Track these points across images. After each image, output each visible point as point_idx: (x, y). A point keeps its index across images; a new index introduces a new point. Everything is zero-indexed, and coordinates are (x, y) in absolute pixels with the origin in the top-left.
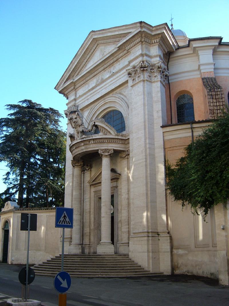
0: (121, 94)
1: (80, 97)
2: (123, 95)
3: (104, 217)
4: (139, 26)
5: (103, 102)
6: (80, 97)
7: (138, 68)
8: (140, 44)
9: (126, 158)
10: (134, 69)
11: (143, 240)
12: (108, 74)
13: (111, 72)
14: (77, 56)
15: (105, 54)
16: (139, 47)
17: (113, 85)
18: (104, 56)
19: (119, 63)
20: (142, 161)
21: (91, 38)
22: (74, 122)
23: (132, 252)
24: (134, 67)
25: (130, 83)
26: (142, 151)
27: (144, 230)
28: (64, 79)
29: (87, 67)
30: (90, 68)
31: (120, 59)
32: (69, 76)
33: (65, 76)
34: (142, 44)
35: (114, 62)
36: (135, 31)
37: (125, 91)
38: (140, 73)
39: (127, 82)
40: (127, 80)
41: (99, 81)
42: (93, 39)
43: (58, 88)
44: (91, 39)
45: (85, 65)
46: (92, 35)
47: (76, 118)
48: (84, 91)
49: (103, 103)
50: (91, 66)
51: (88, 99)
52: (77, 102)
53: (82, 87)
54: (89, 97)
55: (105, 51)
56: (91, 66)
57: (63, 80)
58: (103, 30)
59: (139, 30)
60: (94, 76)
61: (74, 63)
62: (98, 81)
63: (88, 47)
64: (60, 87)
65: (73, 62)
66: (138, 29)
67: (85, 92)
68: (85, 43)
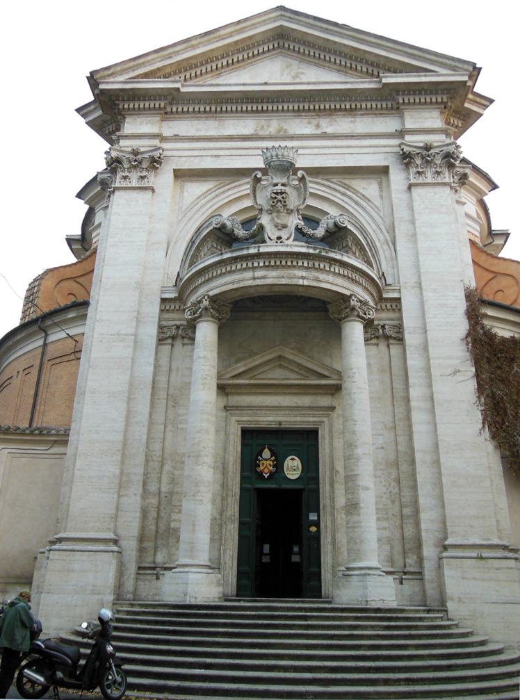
0: (348, 187)
1: (176, 138)
2: (356, 192)
3: (367, 489)
4: (466, 70)
6: (176, 138)
7: (438, 154)
8: (439, 108)
9: (375, 344)
10: (425, 152)
11: (502, 568)
12: (306, 127)
13: (318, 126)
14: (212, 36)
15: (304, 80)
16: (436, 114)
17: (329, 156)
18: (297, 80)
19: (353, 119)
21: (275, 21)
22: (277, 193)
24: (428, 148)
25: (397, 178)
27: (489, 539)
28: (139, 66)
29: (222, 78)
32: (159, 69)
33: (148, 62)
34: (441, 113)
35: (340, 109)
36: (444, 76)
37: (366, 187)
38: (441, 167)
39: (385, 171)
40: (387, 167)
41: (271, 129)
42: (281, 25)
43: (102, 77)
45: (217, 71)
46: (281, 15)
47: (283, 185)
48: (198, 130)
52: (165, 146)
53: (193, 117)
54: (221, 153)
55: (303, 73)
57: (132, 68)
58: (336, 24)
59: (466, 78)
60: (257, 111)
61: (194, 47)
62: (263, 127)
63: (254, 35)
64: (112, 80)
65: (194, 42)
66: (463, 75)
68: (253, 22)
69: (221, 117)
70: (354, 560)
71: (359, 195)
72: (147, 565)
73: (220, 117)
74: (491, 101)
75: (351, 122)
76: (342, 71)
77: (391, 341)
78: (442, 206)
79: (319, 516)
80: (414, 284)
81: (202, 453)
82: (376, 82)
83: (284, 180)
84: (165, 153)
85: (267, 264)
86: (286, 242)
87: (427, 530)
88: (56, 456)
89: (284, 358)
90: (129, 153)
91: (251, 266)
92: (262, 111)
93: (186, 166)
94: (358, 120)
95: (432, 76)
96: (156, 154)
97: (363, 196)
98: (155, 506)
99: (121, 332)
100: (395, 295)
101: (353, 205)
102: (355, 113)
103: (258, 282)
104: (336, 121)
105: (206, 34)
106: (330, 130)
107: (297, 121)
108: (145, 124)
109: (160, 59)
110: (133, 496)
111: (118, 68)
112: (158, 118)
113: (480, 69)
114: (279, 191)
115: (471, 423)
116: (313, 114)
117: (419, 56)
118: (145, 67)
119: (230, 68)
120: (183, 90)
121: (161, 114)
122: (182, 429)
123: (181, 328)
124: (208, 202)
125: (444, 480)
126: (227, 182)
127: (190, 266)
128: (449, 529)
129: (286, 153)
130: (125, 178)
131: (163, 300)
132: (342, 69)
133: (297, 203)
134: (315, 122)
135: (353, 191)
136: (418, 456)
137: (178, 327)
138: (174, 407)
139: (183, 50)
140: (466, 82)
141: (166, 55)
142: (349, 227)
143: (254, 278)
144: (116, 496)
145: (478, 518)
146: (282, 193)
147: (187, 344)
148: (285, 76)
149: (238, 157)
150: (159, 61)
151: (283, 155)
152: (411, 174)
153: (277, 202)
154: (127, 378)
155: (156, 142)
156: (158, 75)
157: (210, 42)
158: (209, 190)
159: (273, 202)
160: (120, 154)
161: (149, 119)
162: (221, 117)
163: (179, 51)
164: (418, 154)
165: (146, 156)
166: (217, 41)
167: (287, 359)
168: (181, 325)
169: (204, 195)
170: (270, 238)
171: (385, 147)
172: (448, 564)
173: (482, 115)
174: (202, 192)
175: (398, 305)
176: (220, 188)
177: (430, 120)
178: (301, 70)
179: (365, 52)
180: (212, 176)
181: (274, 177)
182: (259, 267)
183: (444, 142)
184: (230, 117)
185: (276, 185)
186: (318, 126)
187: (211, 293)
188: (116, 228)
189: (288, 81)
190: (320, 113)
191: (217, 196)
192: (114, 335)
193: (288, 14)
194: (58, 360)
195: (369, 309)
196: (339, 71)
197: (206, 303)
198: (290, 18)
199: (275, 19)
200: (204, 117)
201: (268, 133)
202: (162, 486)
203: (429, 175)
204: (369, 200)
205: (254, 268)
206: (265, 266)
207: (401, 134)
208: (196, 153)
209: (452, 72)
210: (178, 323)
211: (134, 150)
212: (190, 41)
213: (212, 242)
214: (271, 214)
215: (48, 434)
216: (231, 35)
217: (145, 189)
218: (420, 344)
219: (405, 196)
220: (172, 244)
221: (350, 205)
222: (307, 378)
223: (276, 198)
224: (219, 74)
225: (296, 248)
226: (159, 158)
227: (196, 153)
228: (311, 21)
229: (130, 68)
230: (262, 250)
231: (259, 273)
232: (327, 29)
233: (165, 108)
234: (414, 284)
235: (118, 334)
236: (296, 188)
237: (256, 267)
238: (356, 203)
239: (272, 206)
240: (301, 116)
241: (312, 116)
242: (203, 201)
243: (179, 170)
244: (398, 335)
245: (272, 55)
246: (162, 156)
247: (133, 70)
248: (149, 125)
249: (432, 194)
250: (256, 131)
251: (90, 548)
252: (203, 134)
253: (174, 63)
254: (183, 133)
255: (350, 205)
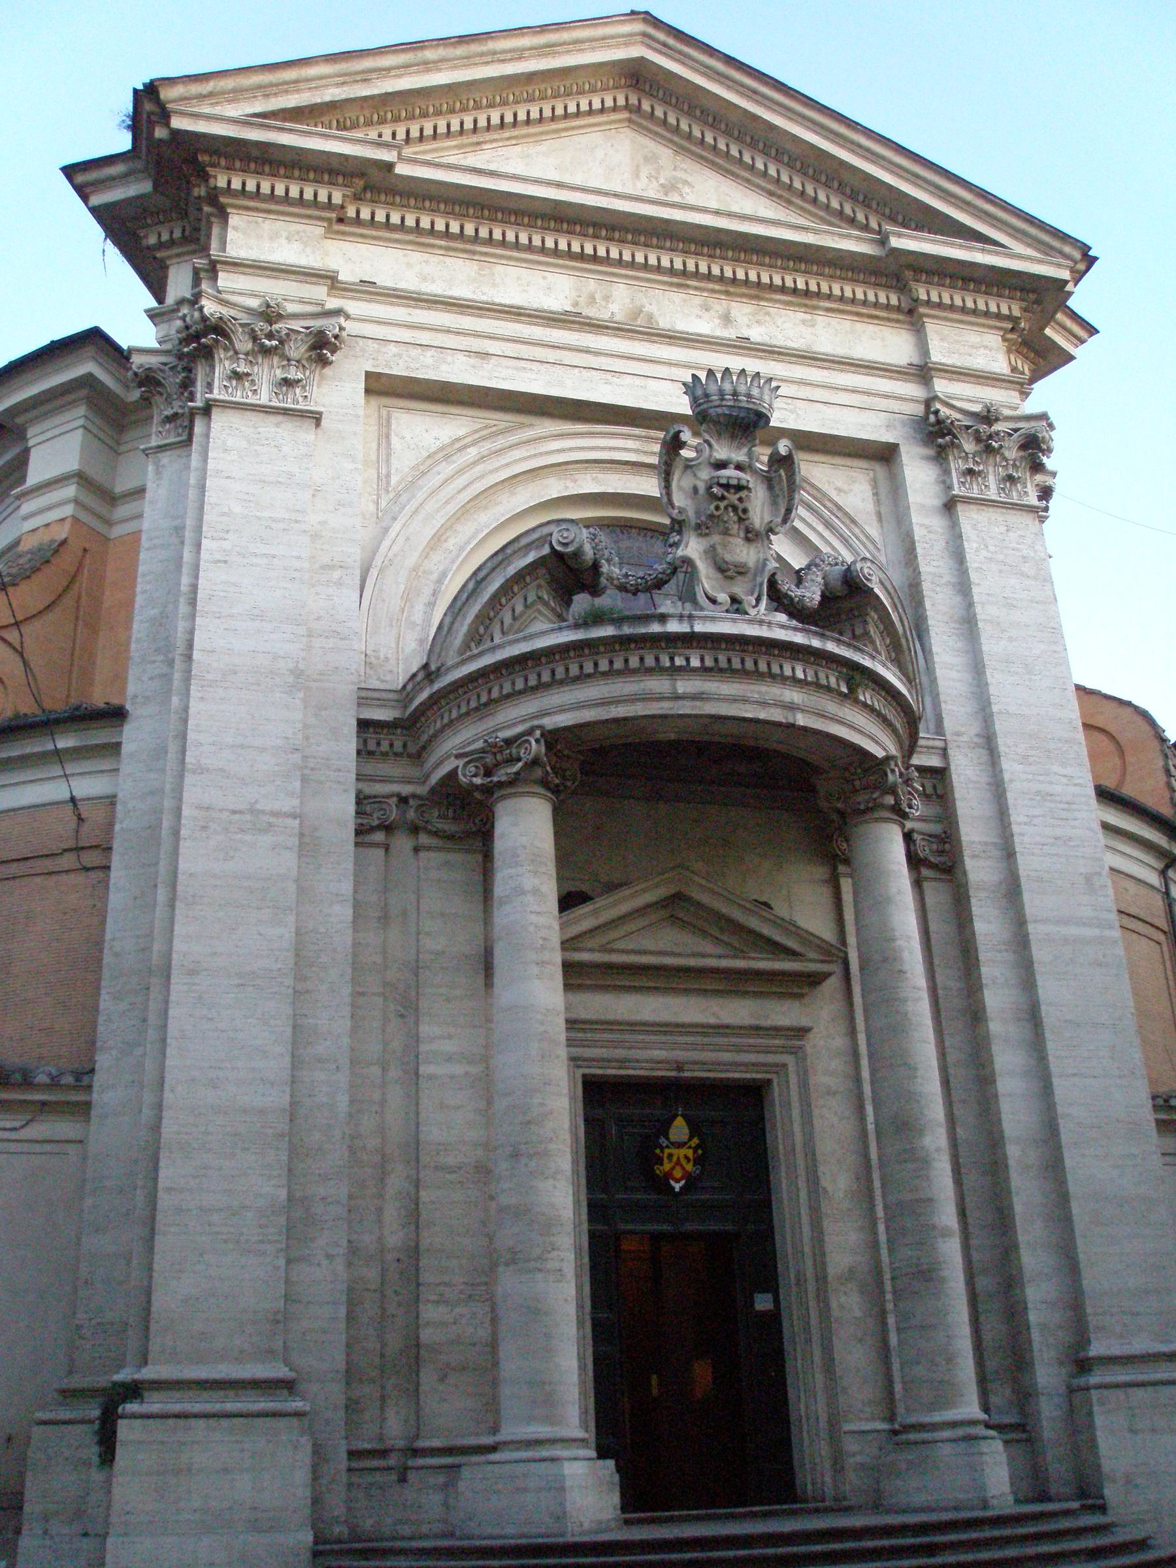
1: (367, 289)
5: (630, 444)
7: (1010, 435)
14: (475, 48)
15: (691, 200)
16: (993, 340)
18: (675, 198)
19: (808, 317)
20: (1096, 932)
21: (626, 44)
22: (727, 487)
23: (1128, 1481)
24: (988, 417)
26: (1088, 879)
30: (492, 174)
31: (827, 304)
32: (332, 106)
33: (308, 80)
37: (845, 487)
38: (1014, 466)
44: (618, 46)
47: (739, 467)
48: (425, 279)
49: (626, 450)
50: (616, 195)
51: (485, 355)
55: (686, 182)
56: (616, 195)
57: (265, 90)
59: (1065, 275)
60: (582, 257)
61: (427, 66)
65: (430, 54)
66: (1059, 266)
67: (456, 292)
69: (486, 254)
70: (933, 1406)
71: (829, 504)
72: (367, 1446)
73: (481, 254)
74: (1097, 332)
75: (804, 322)
76: (780, 197)
77: (925, 872)
78: (1025, 559)
79: (777, 1302)
80: (976, 740)
81: (552, 1146)
82: (872, 241)
83: (740, 456)
84: (351, 327)
85: (709, 662)
86: (753, 612)
87: (1043, 1327)
88: (48, 1147)
89: (688, 899)
90: (249, 311)
91: (668, 664)
92: (595, 258)
93: (399, 369)
94: (821, 320)
95: (997, 253)
96: (330, 326)
97: (839, 508)
98: (373, 1287)
99: (258, 806)
100: (935, 762)
101: (820, 528)
102: (814, 302)
103: (686, 708)
104: (768, 314)
105: (463, 40)
106: (756, 334)
107: (677, 297)
108: (283, 241)
109: (341, 79)
110: (325, 1262)
111: (229, 83)
112: (318, 230)
113: (1095, 259)
114: (734, 482)
115: (1120, 1077)
116: (717, 287)
117: (968, 203)
118: (298, 91)
119: (507, 134)
120: (401, 169)
121: (329, 220)
122: (431, 1077)
123: (411, 802)
124: (460, 472)
125: (1075, 1210)
126: (503, 425)
127: (466, 646)
128: (1093, 1321)
129: (755, 392)
130: (237, 376)
131: (364, 725)
132: (778, 192)
133: (767, 518)
134: (720, 305)
135: (815, 492)
136: (1013, 1152)
137: (403, 800)
138: (402, 1016)
139: (398, 68)
140: (1066, 282)
141: (357, 73)
142: (877, 590)
143: (678, 697)
144: (282, 1262)
145: (1147, 1292)
146: (739, 488)
147: (429, 848)
148: (644, 180)
149: (535, 366)
150: (338, 85)
151: (749, 396)
152: (954, 474)
153: (726, 508)
154: (285, 933)
155: (319, 292)
156: (326, 119)
157: (468, 61)
158: (458, 440)
159: (717, 508)
160: (225, 312)
161: (295, 227)
162: (486, 254)
163: (388, 69)
164: (968, 427)
165: (296, 325)
166: (487, 63)
167: (699, 905)
168: (414, 796)
169: (445, 453)
170: (713, 601)
171: (886, 396)
172: (1102, 1403)
173: (1071, 358)
174: (439, 444)
175: (939, 787)
176: (484, 439)
177: (982, 351)
178: (680, 174)
179: (842, 163)
180: (460, 403)
181: (715, 446)
182: (686, 670)
183: (1016, 409)
184: (510, 258)
185: (721, 465)
186: (727, 319)
187: (549, 722)
188: (223, 514)
189: (652, 194)
190: (731, 286)
191: (482, 459)
192: (241, 812)
193: (661, 36)
194: (14, 869)
195: (910, 793)
196: (771, 194)
197: (535, 748)
198: (665, 45)
199: (628, 40)
200: (440, 247)
201: (606, 316)
202: (386, 1232)
203: (992, 480)
204: (853, 521)
205: (674, 671)
206: (704, 670)
207: (923, 372)
208: (425, 337)
209: (1038, 255)
210: (406, 790)
211: (268, 306)
212: (422, 48)
213: (539, 587)
214: (707, 535)
215: (27, 1082)
216: (519, 55)
217: (302, 415)
218: (1001, 883)
219: (938, 523)
220: (374, 573)
221: (814, 529)
222: (740, 953)
223: (723, 498)
224: (478, 144)
225: (783, 632)
226: (336, 337)
227: (425, 337)
228: (720, 66)
229: (260, 87)
230: (699, 628)
231: (683, 686)
232: (755, 92)
233: (342, 207)
234: (976, 740)
235: (253, 811)
236: (769, 481)
237: (680, 669)
238: (828, 525)
239: (711, 516)
240: (688, 286)
241: (713, 291)
242: (447, 469)
243: (379, 375)
244: (942, 859)
245: (611, 123)
246: (344, 334)
247: (266, 96)
248: (296, 246)
249: (1003, 529)
250: (576, 304)
251: (230, 1407)
252: (439, 291)
253: (372, 97)
254: (385, 280)
255: (814, 529)
